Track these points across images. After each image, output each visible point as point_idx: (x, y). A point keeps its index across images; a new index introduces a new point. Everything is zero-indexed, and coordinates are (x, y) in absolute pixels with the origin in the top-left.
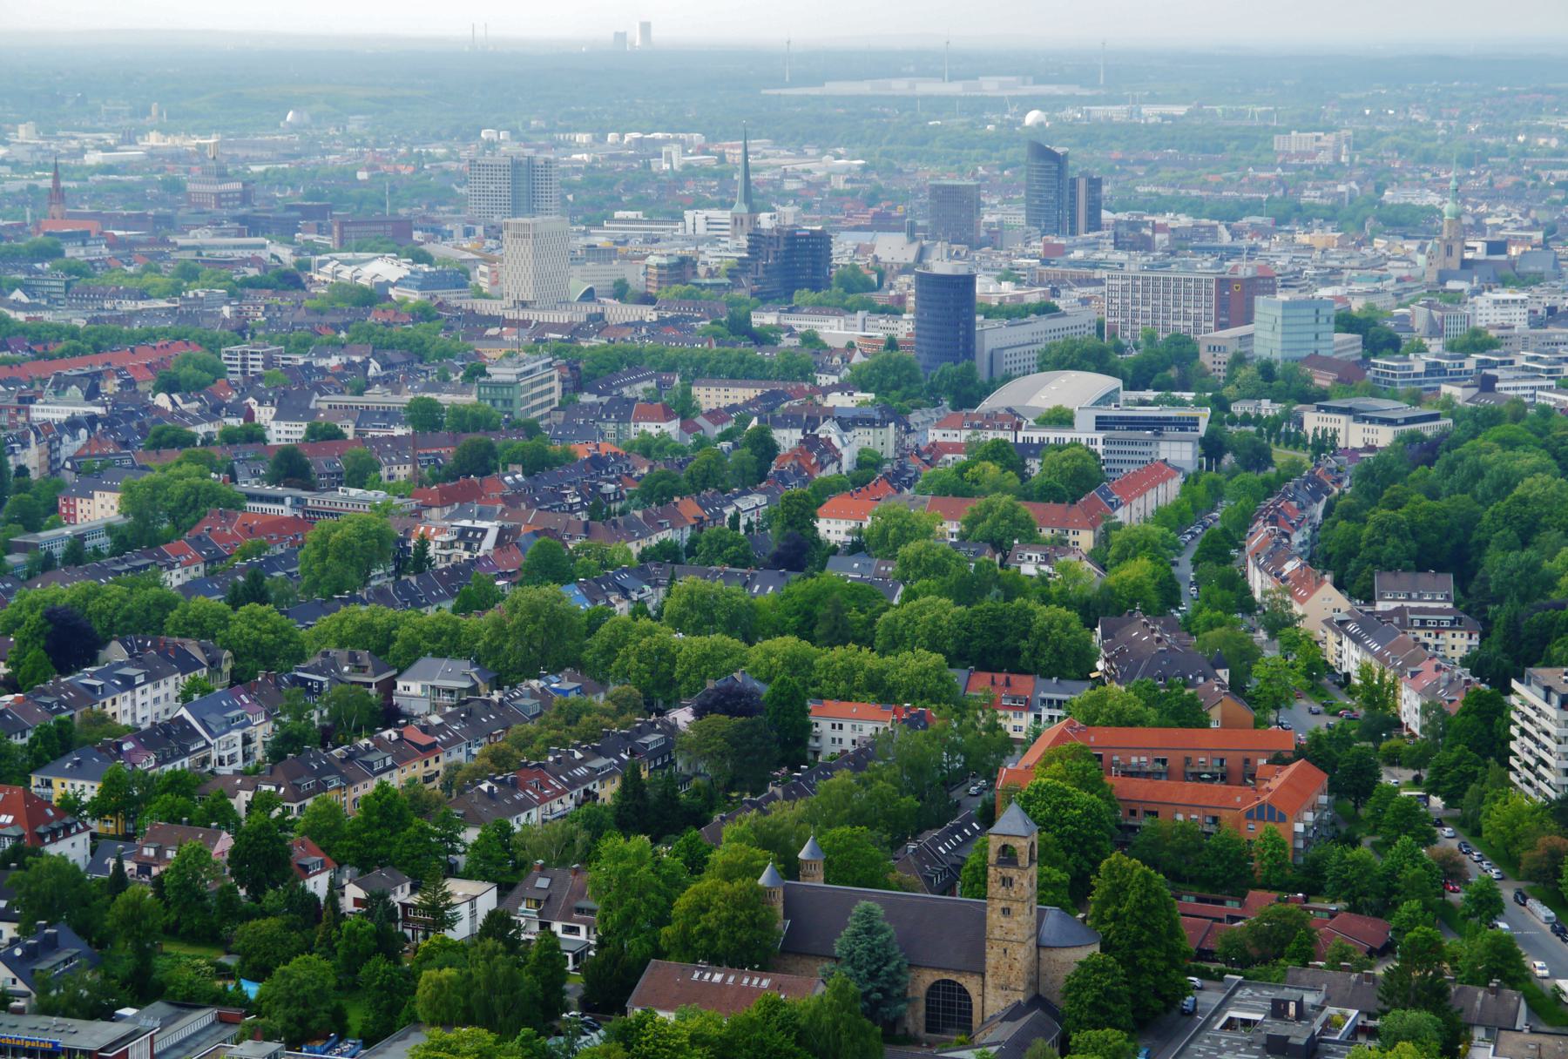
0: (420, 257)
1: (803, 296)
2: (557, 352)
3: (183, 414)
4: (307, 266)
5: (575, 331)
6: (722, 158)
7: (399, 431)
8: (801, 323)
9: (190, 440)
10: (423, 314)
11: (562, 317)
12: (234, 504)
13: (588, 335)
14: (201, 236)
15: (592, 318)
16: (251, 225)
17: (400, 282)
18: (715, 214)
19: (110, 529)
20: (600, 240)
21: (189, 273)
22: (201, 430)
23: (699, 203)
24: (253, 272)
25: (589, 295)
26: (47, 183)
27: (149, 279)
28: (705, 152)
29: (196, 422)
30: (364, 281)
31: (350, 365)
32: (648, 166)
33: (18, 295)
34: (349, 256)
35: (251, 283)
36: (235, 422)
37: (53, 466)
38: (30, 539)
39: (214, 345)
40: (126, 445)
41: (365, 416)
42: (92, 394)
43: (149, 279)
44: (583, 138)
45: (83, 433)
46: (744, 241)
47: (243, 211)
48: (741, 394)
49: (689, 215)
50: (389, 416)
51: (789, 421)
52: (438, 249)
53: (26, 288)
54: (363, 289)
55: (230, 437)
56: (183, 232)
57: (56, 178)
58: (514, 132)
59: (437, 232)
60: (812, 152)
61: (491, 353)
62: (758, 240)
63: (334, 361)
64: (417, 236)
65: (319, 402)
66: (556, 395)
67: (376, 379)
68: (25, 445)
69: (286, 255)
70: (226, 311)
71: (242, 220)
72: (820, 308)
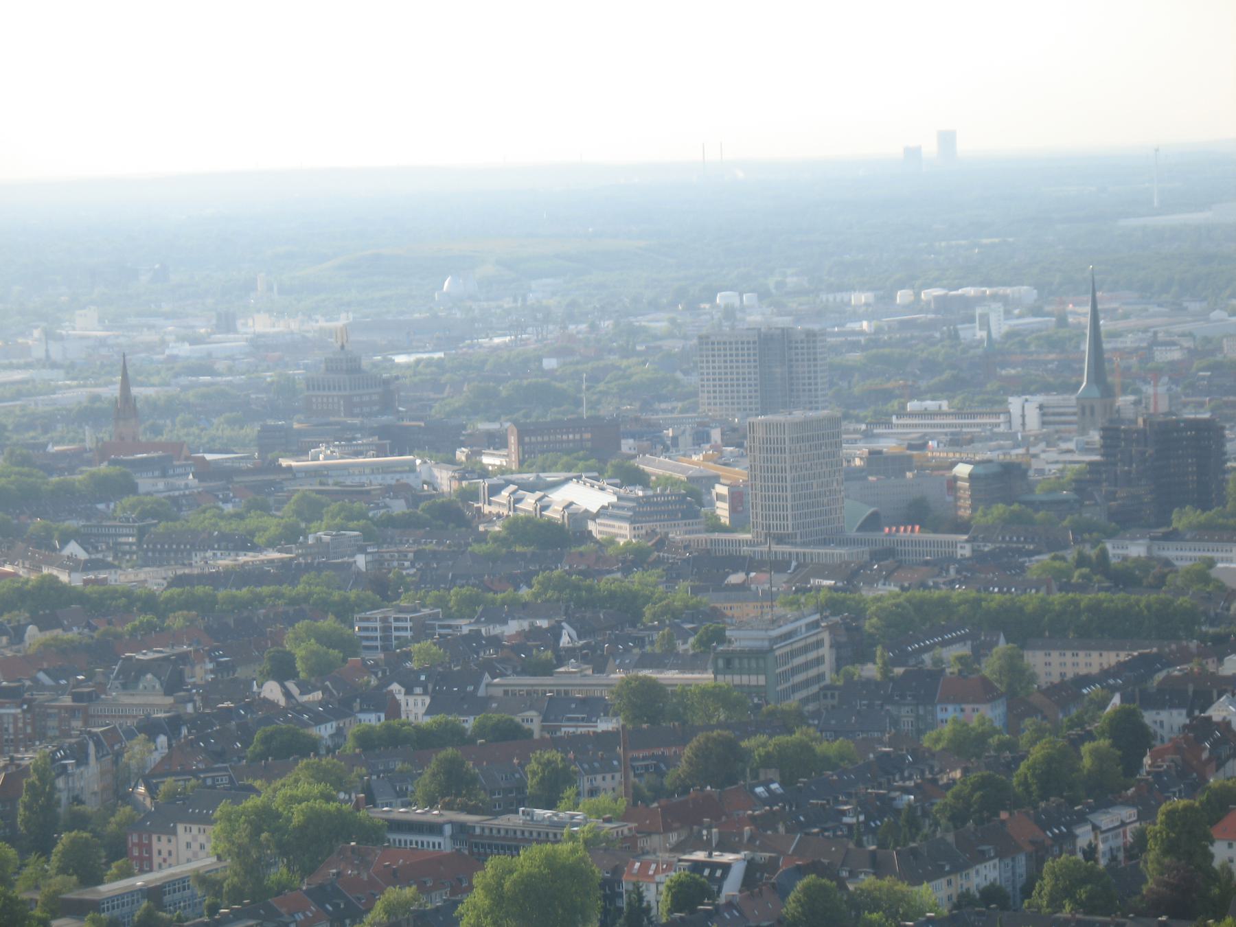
0: (633, 477)
1: (1185, 518)
2: (832, 606)
3: (304, 708)
4: (472, 495)
5: (851, 576)
6: (1062, 321)
7: (605, 725)
8: (1184, 556)
9: (310, 747)
10: (635, 559)
11: (839, 553)
12: (372, 835)
13: (871, 582)
14: (323, 456)
15: (876, 556)
16: (397, 440)
17: (603, 512)
18: (1053, 399)
19: (203, 880)
20: (888, 445)
21: (311, 510)
22: (325, 731)
23: (1024, 388)
24: (399, 507)
25: (873, 522)
26: (112, 391)
27: (252, 521)
28: (1036, 311)
29: (319, 720)
30: (555, 513)
31: (535, 632)
32: (955, 336)
33: (74, 549)
34: (530, 477)
35: (391, 521)
36: (372, 720)
37: (118, 792)
38: (88, 894)
39: (345, 611)
40: (220, 756)
41: (556, 707)
42: (174, 684)
43: (252, 521)
44: (860, 298)
45: (162, 740)
46: (1095, 436)
47: (385, 419)
48: (1095, 661)
49: (1015, 404)
50: (592, 707)
51: (1169, 697)
52: (656, 466)
53: (84, 540)
54: (551, 523)
55: (367, 740)
56: (301, 452)
57: (126, 384)
58: (763, 295)
59: (654, 441)
60: (1194, 306)
61: (737, 610)
62: (1113, 436)
63: (513, 627)
64: (627, 445)
65: (493, 685)
66: (826, 668)
67: (571, 652)
68: (82, 760)
69: (445, 480)
70: (361, 561)
71: (384, 432)
72: (1209, 532)
